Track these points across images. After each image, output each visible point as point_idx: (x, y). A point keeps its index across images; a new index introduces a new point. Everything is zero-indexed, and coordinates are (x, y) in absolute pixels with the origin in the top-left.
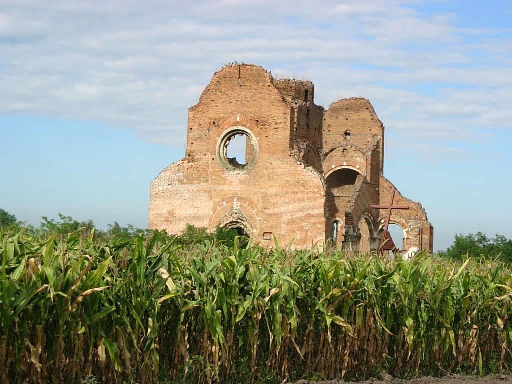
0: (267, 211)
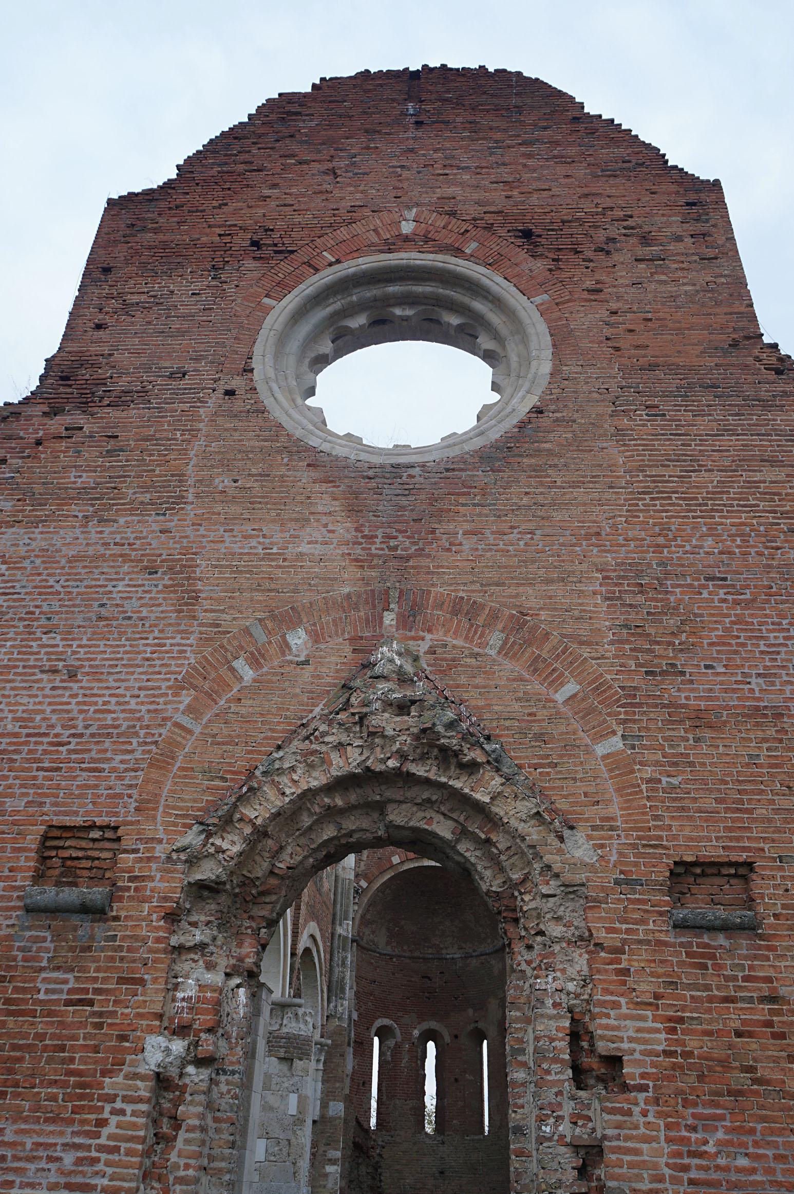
0: (673, 690)
